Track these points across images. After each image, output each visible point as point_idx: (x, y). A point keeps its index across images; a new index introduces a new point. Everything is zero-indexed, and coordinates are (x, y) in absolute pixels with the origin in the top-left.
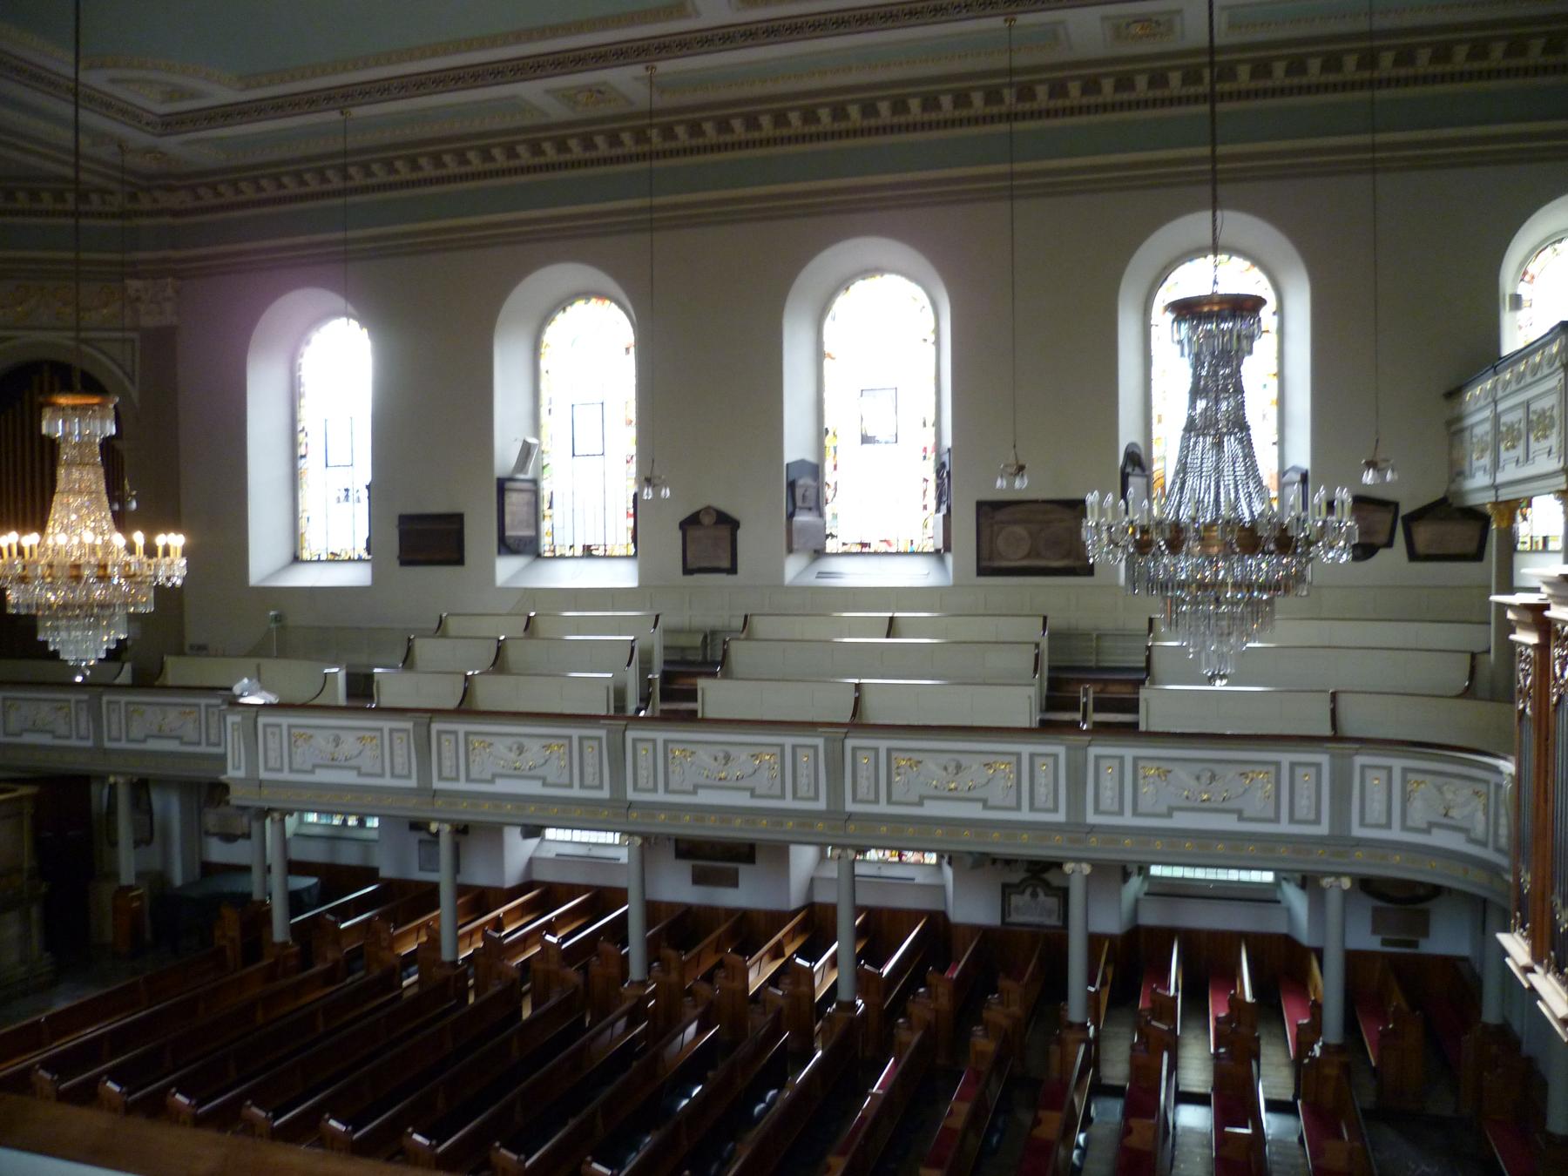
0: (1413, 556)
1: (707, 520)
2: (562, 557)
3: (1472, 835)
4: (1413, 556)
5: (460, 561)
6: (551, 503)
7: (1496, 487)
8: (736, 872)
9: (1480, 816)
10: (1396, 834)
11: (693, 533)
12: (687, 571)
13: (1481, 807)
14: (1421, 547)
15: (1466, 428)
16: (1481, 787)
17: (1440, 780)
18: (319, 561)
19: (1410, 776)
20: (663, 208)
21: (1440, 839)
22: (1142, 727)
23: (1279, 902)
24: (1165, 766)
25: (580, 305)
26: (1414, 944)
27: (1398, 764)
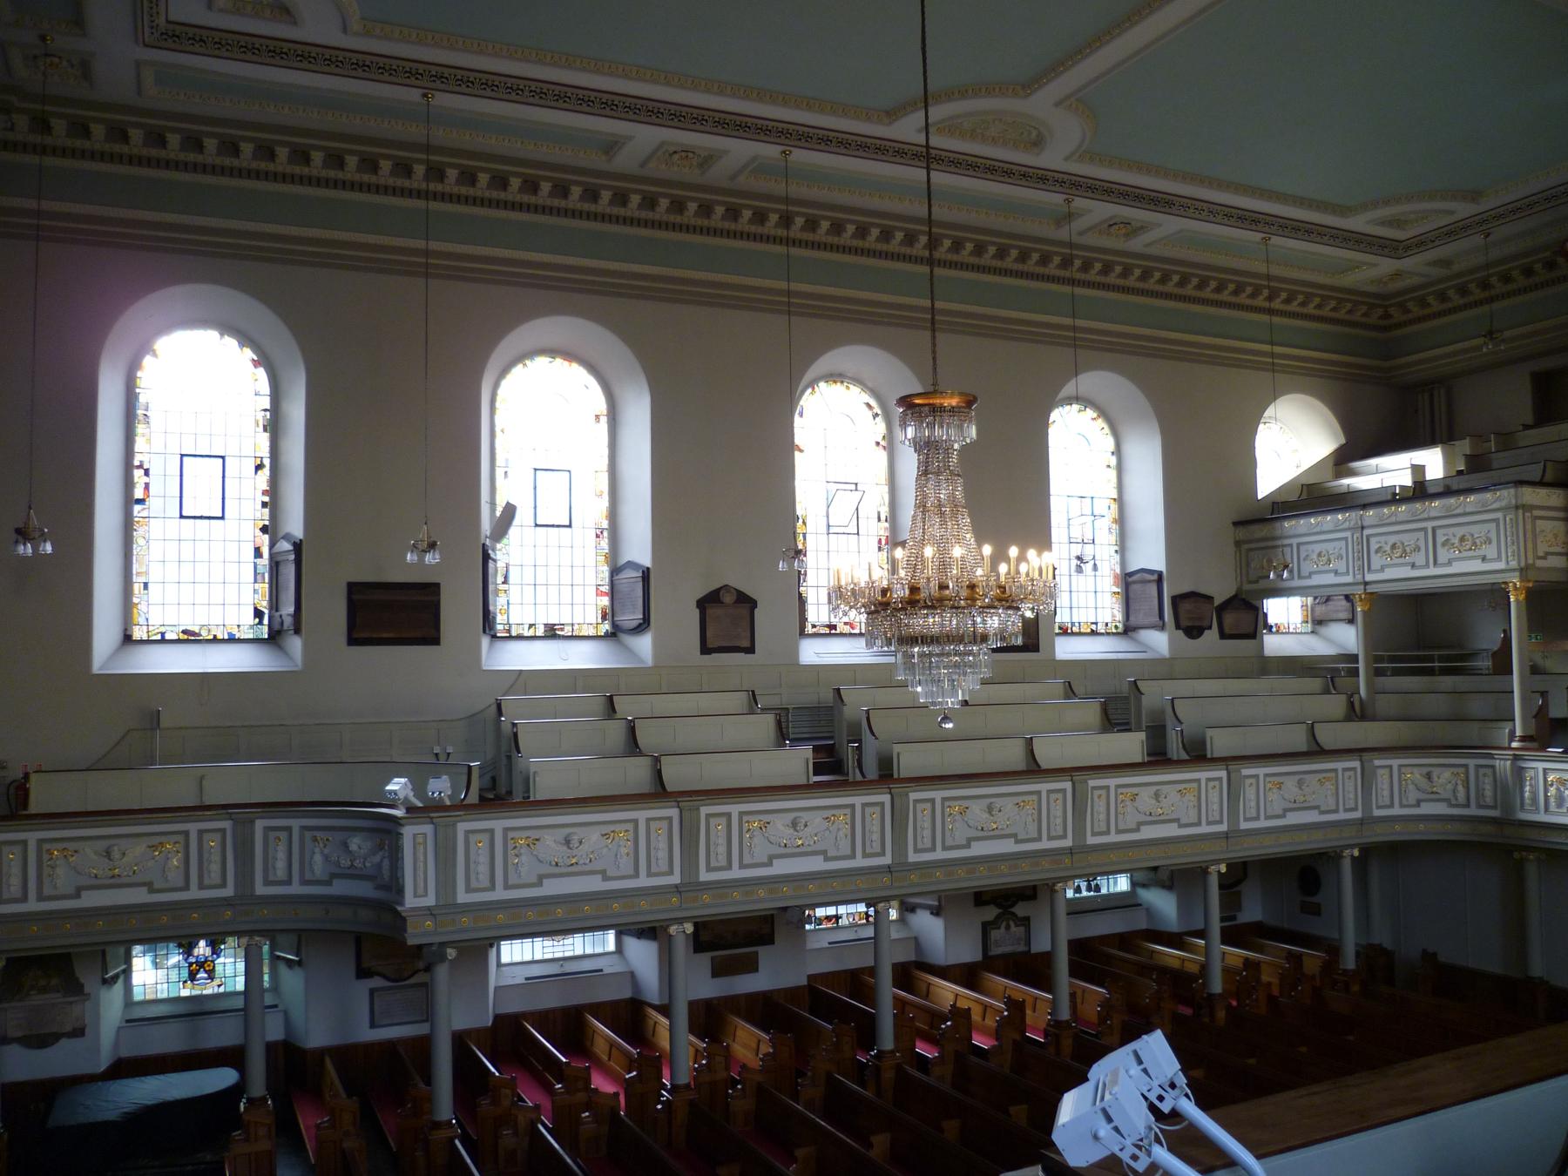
0: (1223, 636)
1: (728, 599)
2: (520, 637)
3: (1454, 802)
4: (1223, 636)
5: (435, 641)
6: (506, 577)
7: (1366, 583)
8: (757, 953)
9: (1460, 788)
10: (1397, 811)
11: (712, 611)
12: (705, 650)
13: (1459, 782)
14: (1227, 630)
15: (1291, 545)
16: (1462, 770)
17: (1425, 770)
18: (163, 641)
19: (1403, 770)
20: (799, 294)
21: (1428, 809)
22: (1209, 756)
23: (1140, 905)
24: (1277, 779)
25: (542, 362)
26: (1234, 918)
27: (1395, 763)
